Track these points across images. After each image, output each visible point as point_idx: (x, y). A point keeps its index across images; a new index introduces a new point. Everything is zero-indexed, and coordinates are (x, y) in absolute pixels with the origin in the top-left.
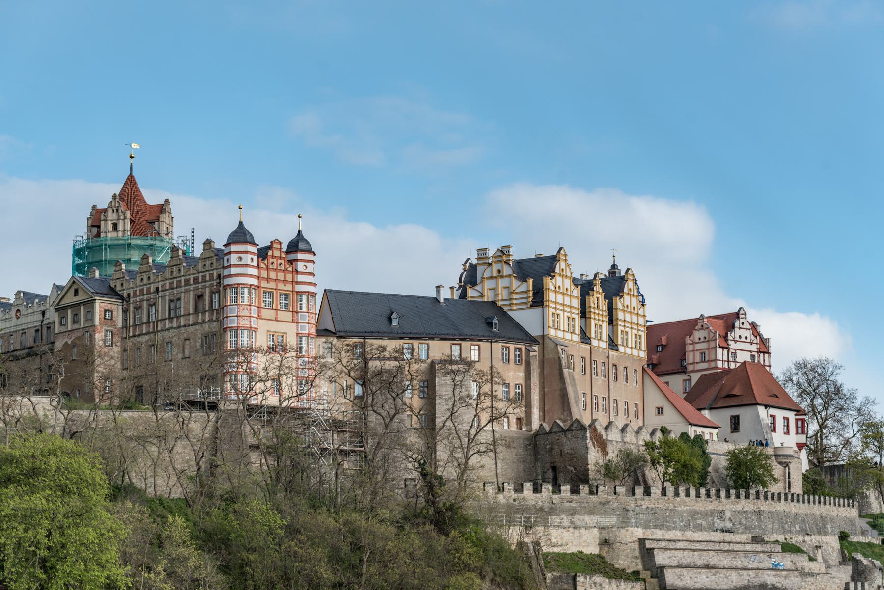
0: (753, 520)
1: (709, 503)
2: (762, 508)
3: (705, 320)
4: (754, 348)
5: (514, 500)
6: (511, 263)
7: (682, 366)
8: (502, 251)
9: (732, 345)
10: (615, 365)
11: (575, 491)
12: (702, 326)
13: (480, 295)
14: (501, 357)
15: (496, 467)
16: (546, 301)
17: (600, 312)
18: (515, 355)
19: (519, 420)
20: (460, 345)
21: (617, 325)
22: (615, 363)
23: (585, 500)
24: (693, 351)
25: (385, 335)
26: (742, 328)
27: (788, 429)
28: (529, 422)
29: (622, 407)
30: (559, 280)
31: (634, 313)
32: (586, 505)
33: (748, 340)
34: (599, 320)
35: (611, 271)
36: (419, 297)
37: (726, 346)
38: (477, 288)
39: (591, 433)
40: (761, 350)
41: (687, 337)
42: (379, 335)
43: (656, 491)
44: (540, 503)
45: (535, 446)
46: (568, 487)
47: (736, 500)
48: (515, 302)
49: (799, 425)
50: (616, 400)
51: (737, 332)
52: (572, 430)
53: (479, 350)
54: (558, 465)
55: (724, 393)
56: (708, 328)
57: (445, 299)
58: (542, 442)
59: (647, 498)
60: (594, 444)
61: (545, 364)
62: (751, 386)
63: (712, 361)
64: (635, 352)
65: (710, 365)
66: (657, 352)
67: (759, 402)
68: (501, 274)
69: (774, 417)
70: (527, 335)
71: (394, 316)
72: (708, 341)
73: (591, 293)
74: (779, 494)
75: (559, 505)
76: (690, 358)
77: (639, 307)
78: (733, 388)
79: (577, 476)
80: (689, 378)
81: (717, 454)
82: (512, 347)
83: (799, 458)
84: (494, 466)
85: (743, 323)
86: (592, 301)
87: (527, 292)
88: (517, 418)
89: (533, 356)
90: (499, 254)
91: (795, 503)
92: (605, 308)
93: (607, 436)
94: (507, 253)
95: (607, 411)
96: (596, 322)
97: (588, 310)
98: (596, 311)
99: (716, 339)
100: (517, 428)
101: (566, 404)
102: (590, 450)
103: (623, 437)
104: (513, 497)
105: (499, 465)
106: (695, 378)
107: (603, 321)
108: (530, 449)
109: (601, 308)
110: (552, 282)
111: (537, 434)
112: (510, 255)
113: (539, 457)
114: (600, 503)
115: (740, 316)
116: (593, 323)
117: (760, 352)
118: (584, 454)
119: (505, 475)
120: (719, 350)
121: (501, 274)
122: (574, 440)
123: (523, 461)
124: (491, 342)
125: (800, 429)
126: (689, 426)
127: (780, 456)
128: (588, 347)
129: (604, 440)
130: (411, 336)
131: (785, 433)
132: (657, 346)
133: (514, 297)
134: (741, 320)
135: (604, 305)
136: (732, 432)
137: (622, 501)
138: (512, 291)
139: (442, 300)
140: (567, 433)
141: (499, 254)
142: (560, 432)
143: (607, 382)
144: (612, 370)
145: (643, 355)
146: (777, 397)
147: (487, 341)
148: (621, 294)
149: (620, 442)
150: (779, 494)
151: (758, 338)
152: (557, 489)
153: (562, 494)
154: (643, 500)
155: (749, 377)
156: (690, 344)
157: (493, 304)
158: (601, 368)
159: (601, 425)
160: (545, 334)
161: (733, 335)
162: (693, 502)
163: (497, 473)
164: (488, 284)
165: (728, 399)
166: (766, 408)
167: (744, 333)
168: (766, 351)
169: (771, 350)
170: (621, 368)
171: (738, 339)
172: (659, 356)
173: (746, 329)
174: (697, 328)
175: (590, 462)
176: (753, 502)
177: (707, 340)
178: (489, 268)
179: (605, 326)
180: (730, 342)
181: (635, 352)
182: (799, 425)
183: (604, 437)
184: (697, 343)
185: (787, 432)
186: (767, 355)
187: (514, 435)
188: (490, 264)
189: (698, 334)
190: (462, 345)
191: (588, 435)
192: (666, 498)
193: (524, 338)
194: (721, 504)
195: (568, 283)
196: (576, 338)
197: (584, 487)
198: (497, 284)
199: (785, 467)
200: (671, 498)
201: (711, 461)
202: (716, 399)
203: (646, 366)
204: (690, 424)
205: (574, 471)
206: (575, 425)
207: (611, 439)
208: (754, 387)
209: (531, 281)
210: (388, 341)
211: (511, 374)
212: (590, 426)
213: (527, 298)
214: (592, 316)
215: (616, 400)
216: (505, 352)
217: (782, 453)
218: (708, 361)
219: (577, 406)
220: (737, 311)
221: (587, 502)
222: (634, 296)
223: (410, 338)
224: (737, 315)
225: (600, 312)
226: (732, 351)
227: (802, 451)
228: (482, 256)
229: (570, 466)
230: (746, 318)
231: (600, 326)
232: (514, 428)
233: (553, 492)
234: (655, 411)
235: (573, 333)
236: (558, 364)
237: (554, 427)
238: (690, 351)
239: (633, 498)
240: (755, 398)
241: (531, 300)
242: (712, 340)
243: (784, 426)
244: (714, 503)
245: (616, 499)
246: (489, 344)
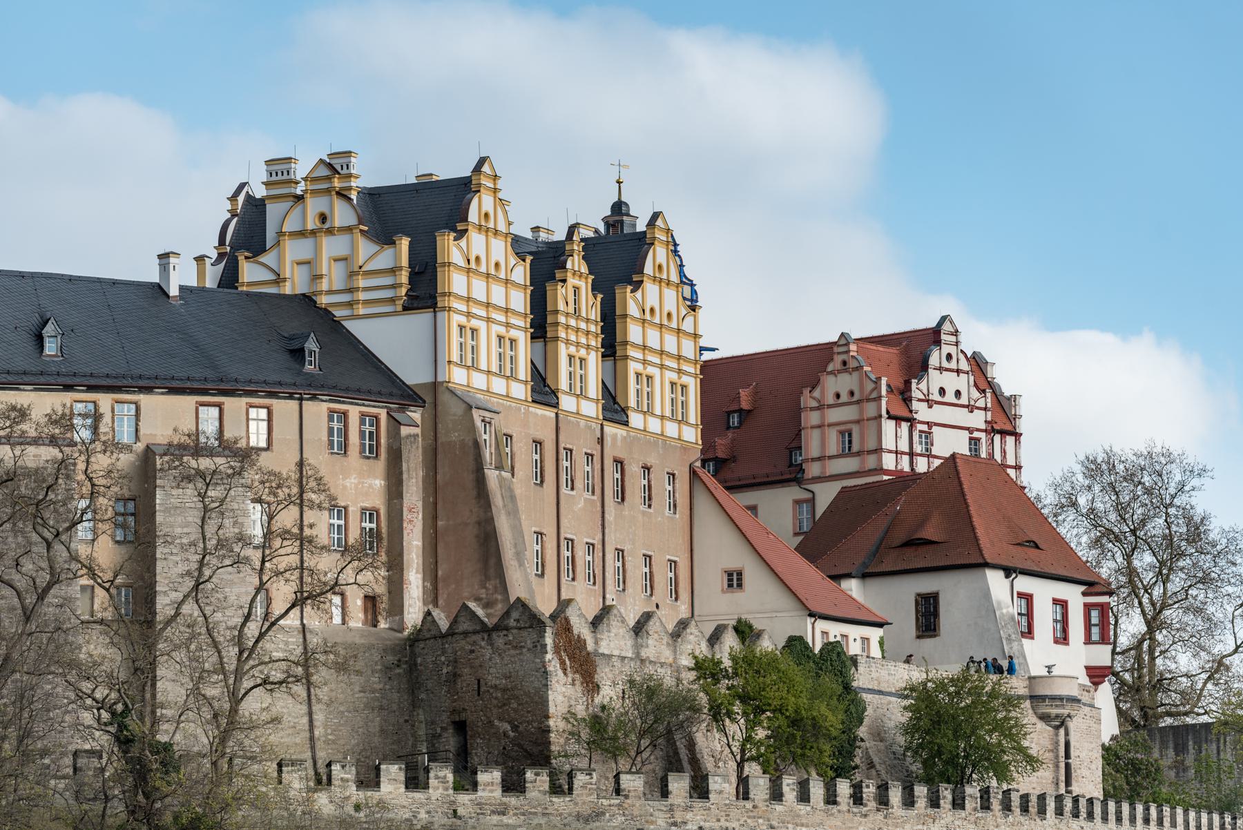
1: (858, 819)
3: (853, 347)
4: (978, 420)
5: (357, 808)
6: (354, 196)
7: (791, 465)
8: (330, 166)
9: (922, 412)
10: (619, 462)
11: (513, 785)
12: (844, 363)
13: (272, 277)
14: (325, 438)
15: (311, 721)
16: (444, 294)
17: (583, 325)
18: (362, 434)
19: (371, 601)
20: (220, 406)
21: (626, 357)
22: (621, 455)
23: (540, 809)
24: (819, 427)
25: (26, 379)
26: (947, 370)
27: (1065, 630)
28: (397, 607)
29: (637, 570)
30: (476, 241)
31: (670, 329)
32: (543, 821)
33: (964, 401)
34: (578, 344)
35: (611, 220)
36: (114, 283)
37: (908, 415)
38: (264, 259)
39: (556, 635)
40: (997, 427)
41: (806, 391)
42: (10, 378)
43: (722, 785)
44: (423, 815)
45: (413, 667)
46: (496, 775)
47: (930, 811)
48: (362, 296)
49: (1095, 620)
50: (620, 552)
51: (935, 380)
52: (507, 629)
53: (270, 420)
54: (470, 717)
55: (900, 536)
56: (859, 368)
57: (182, 288)
58: (430, 659)
59: (698, 804)
60: (562, 663)
61: (439, 457)
62: (970, 517)
63: (870, 452)
64: (672, 429)
65: (863, 462)
66: (728, 428)
67: (989, 561)
68: (327, 226)
69: (1028, 598)
70: (393, 382)
71: (49, 329)
72: (858, 402)
73: (559, 275)
74: (1042, 798)
75: (471, 822)
76: (812, 444)
77: (683, 311)
78: (921, 524)
79: (520, 745)
80: (810, 495)
81: (880, 692)
82: (354, 412)
83: (1092, 706)
84: (305, 720)
85: (949, 357)
86: (561, 297)
87: (393, 271)
88: (366, 597)
89: (409, 436)
90: (324, 172)
91: (1082, 821)
92: (595, 314)
93: (596, 643)
94: (345, 171)
95: (597, 578)
96: (572, 349)
97: (550, 319)
98: (573, 322)
99: (880, 397)
100: (365, 622)
101: (492, 561)
102: (554, 680)
103: (637, 647)
104: (354, 799)
105: (319, 717)
106: (826, 495)
107: (588, 347)
108: (399, 674)
109: (584, 314)
110: (460, 248)
111: (417, 637)
112: (350, 176)
113: (423, 696)
114: (578, 817)
115: (943, 337)
116: (563, 351)
117: (994, 431)
118: (537, 691)
119: (334, 742)
120: (888, 426)
121: (327, 226)
122: (513, 652)
123: (381, 708)
124: (301, 399)
125: (1095, 631)
126: (810, 620)
127: (1043, 698)
128: (550, 413)
129: (588, 654)
130: (93, 382)
131: (1056, 641)
132: (729, 413)
133: (362, 283)
134: (946, 349)
135: (591, 307)
136: (918, 637)
137: (636, 812)
138: (356, 269)
139: (174, 291)
140: (494, 635)
141: (324, 172)
142: (475, 632)
143: (599, 504)
144: (611, 475)
145: (691, 435)
146: (1037, 547)
147: (291, 397)
148: (636, 278)
149: (631, 659)
150: (1042, 798)
151: (989, 395)
152: (466, 781)
153: (480, 793)
154: (688, 808)
155: (963, 495)
156: (812, 409)
157: (307, 300)
158: (582, 467)
159: (582, 615)
160: (440, 379)
161: (923, 386)
162: (819, 816)
163: (312, 739)
164: (294, 250)
165: (909, 552)
166: (1007, 576)
167: (952, 382)
168: (1008, 427)
169: (1023, 426)
170: (634, 469)
171: (936, 396)
172: (733, 440)
173: (958, 371)
174: (830, 368)
175: (552, 710)
176: (972, 819)
177: (856, 398)
178: (297, 210)
179: (594, 360)
180: (915, 405)
181: (672, 429)
182: (1095, 620)
183: (590, 646)
184: (830, 406)
185: (1063, 638)
186: (1010, 440)
187: (358, 640)
188: (299, 198)
189: (835, 384)
190: (226, 407)
191: (549, 640)
192: (749, 805)
193: (384, 390)
194: (890, 822)
195: (499, 250)
196: (520, 391)
197: (537, 774)
198: (317, 250)
199: (1057, 728)
200: (762, 805)
201: (865, 709)
202: (878, 551)
203: (698, 464)
204: (811, 615)
205: (512, 734)
206: (515, 615)
207: (606, 652)
208: (977, 521)
209: (405, 243)
210: (33, 394)
211: (351, 481)
212: (553, 617)
213: (394, 287)
214: (562, 334)
215: (620, 552)
216: (336, 425)
217: (1048, 693)
218: (858, 454)
219: (521, 564)
220: (933, 324)
221: (544, 814)
222: (669, 283)
223: (91, 388)
224: (933, 336)
225: (583, 325)
226: (920, 427)
227: (1101, 687)
228: (280, 177)
229: (500, 719)
230: (957, 344)
231: (582, 360)
232: (357, 620)
233: (458, 788)
234: (720, 581)
235: (512, 377)
236: (471, 458)
237: (462, 619)
238: (812, 427)
239: (662, 804)
240: (980, 550)
241: (404, 291)
242: (868, 400)
243: (1055, 621)
244: (871, 818)
245: (619, 805)
246: (293, 405)
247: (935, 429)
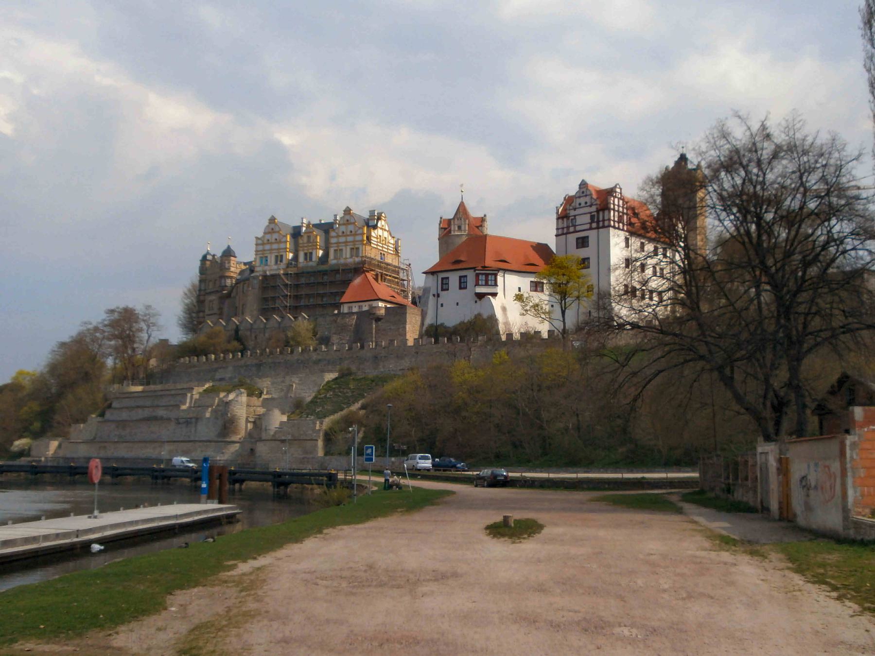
33: (588, 204)
171: (578, 206)
247: (577, 217)
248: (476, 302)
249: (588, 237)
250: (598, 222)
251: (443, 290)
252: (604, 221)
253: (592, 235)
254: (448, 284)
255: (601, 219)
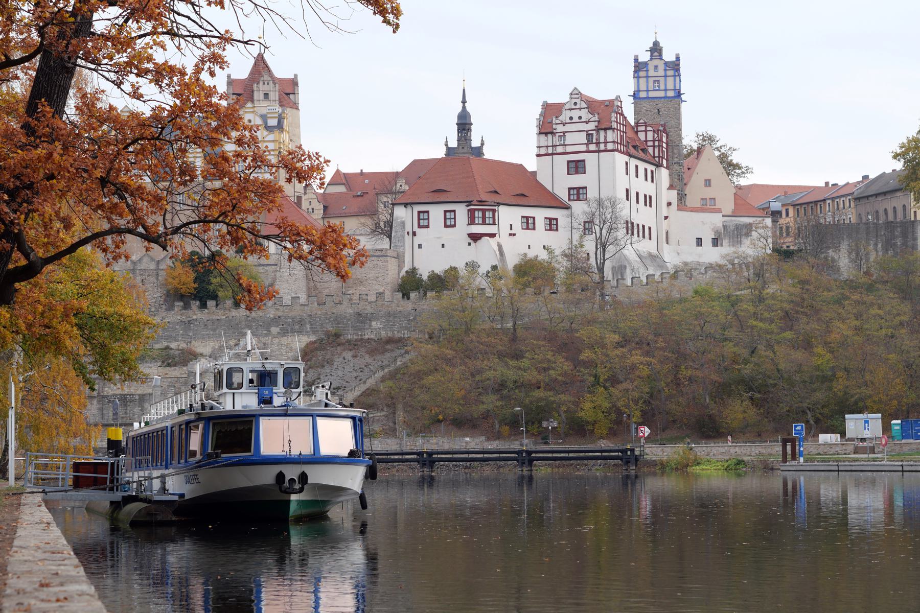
0: (176, 329)
2: (195, 317)
4: (592, 126)
167: (575, 114)
248: (469, 244)
249: (584, 161)
250: (598, 143)
251: (419, 227)
252: (606, 143)
253: (591, 160)
254: (428, 219)
255: (602, 140)
